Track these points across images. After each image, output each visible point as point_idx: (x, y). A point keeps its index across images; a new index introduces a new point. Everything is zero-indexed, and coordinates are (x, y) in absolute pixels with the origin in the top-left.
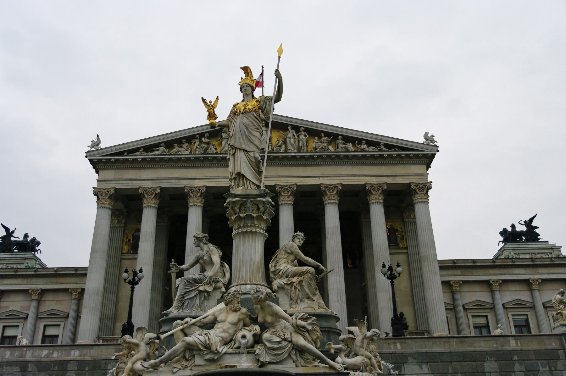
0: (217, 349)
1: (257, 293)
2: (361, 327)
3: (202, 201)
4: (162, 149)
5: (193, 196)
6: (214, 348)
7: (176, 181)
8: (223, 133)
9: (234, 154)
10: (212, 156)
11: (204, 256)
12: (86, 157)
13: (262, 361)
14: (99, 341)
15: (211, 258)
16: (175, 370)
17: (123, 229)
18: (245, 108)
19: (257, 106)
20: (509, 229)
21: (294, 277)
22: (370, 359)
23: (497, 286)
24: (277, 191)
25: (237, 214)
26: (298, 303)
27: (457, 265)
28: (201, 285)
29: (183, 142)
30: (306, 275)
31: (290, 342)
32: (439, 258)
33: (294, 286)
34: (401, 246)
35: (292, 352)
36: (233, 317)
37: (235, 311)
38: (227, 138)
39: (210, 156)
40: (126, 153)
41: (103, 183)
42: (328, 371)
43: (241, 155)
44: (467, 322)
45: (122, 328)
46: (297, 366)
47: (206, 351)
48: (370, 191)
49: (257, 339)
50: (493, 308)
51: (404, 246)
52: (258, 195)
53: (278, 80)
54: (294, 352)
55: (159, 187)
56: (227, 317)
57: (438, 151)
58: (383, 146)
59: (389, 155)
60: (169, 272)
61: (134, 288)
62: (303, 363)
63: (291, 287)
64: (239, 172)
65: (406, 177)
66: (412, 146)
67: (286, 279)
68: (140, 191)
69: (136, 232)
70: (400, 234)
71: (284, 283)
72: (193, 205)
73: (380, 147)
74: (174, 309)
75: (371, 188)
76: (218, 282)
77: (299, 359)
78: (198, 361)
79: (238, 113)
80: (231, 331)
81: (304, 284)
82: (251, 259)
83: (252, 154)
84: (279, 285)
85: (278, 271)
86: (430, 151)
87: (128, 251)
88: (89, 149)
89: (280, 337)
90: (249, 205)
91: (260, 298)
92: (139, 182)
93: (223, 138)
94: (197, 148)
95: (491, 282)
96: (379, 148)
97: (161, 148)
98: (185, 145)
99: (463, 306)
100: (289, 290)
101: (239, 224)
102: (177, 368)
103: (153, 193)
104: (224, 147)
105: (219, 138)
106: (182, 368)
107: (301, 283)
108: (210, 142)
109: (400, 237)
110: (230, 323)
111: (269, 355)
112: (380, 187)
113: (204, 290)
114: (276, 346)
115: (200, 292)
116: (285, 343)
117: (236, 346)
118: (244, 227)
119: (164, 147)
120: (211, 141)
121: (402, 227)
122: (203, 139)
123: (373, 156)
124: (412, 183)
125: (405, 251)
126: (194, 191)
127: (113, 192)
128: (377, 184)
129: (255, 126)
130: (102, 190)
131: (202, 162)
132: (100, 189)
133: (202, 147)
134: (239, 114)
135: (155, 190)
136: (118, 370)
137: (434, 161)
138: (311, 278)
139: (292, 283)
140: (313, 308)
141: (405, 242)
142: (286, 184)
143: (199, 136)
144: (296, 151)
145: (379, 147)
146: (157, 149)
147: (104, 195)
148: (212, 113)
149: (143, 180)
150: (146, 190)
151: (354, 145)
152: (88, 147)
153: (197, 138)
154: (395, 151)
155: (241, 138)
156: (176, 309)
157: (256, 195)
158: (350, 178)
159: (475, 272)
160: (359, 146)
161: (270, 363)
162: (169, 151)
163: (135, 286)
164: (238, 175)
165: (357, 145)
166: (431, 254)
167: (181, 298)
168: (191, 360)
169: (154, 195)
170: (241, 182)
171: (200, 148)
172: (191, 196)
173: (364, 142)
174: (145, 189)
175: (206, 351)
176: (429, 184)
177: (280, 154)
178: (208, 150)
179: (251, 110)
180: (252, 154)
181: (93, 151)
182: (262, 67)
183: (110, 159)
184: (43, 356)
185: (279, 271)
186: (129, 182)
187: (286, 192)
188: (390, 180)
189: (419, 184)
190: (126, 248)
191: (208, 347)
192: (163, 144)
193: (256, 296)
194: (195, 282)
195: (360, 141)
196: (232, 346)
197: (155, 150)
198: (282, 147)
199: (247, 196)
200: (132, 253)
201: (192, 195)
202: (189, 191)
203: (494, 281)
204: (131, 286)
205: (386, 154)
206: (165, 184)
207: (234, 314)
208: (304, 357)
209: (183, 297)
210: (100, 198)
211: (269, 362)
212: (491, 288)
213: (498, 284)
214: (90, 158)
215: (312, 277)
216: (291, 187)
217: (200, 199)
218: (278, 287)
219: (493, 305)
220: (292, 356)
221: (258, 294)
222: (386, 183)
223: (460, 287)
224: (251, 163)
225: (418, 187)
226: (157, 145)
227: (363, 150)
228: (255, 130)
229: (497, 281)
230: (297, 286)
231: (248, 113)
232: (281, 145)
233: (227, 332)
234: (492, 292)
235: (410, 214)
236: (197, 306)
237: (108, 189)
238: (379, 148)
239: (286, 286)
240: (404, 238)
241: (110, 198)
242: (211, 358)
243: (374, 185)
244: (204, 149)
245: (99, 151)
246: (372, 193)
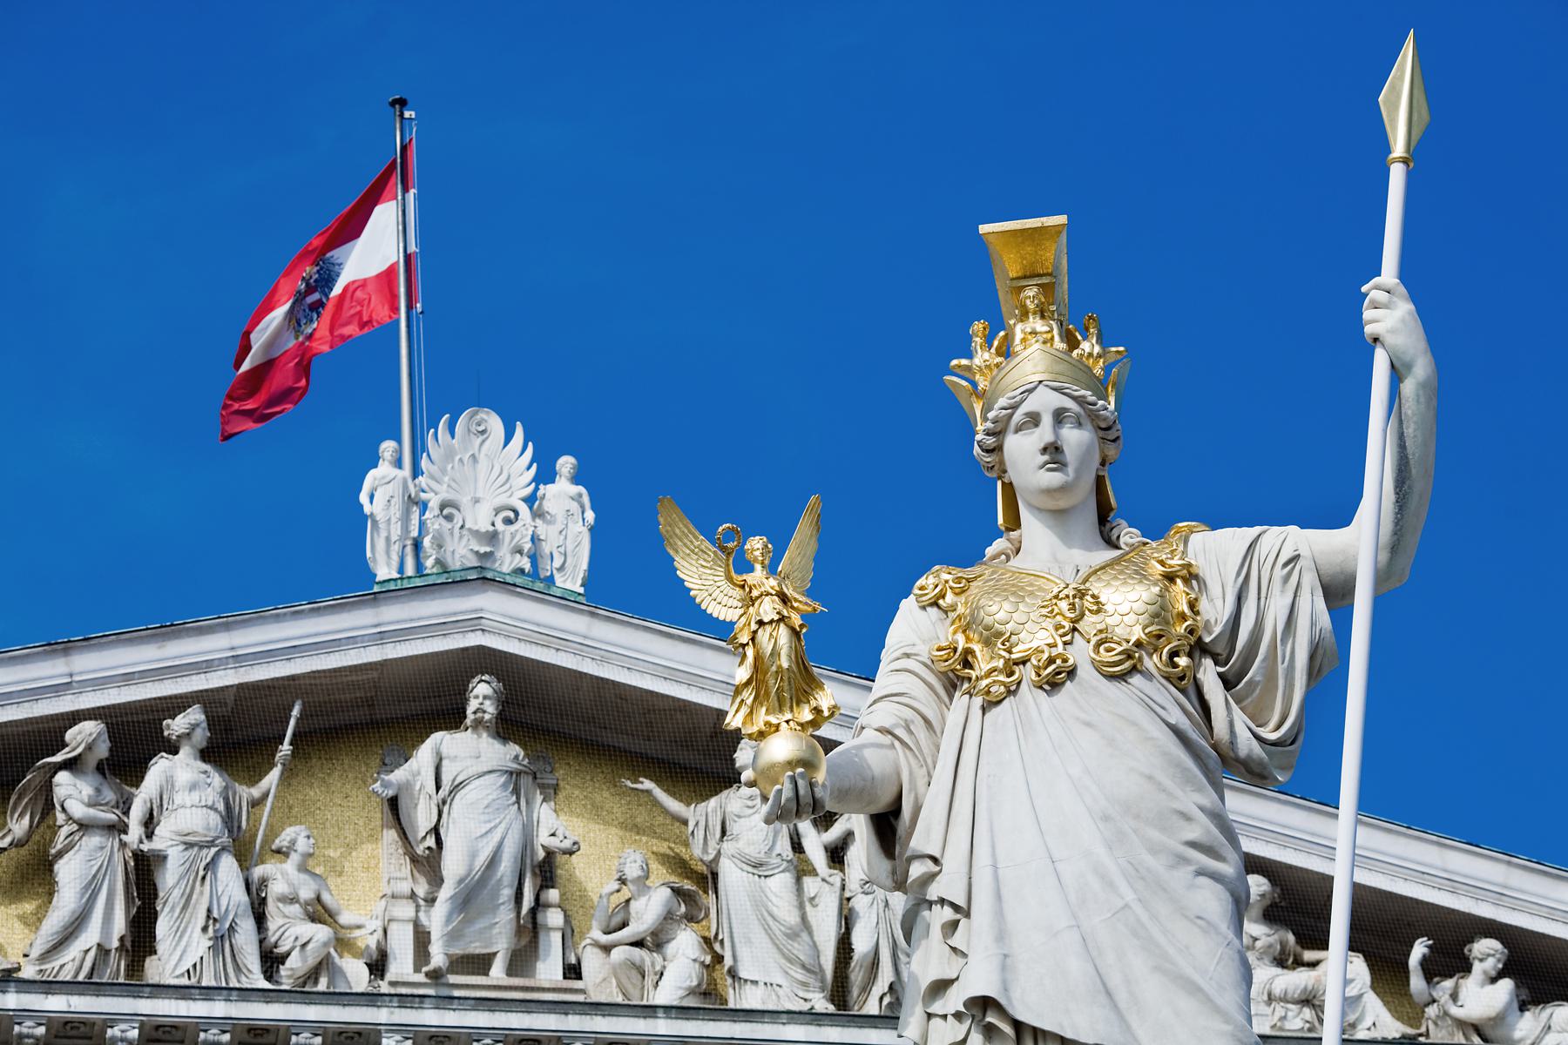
8: (70, 765)
79: (1002, 678)
105: (26, 821)
144: (822, 1004)
198: (670, 949)
228: (1185, 860)
232: (654, 934)
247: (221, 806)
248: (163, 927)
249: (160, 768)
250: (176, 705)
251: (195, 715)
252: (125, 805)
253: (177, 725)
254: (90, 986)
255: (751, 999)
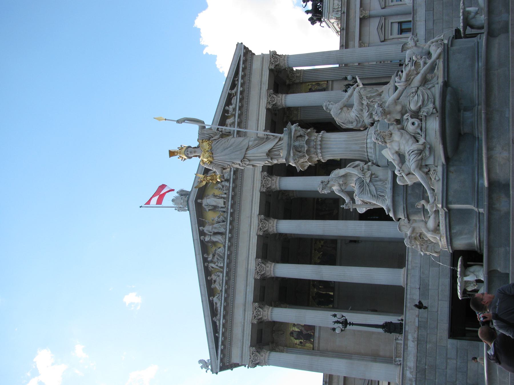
0: (422, 145)
1: (378, 113)
2: (407, 48)
3: (270, 263)
4: (215, 299)
5: (264, 272)
6: (421, 147)
7: (248, 287)
8: (205, 240)
9: (249, 160)
10: (226, 251)
11: (339, 184)
12: (217, 373)
13: (432, 109)
14: (397, 361)
15: (342, 176)
16: (437, 178)
17: (289, 348)
18: (208, 151)
19: (206, 141)
20: (310, 15)
21: (363, 104)
22: (432, 43)
23: (365, 12)
24: (266, 190)
25: (304, 154)
26: (385, 101)
27: (344, 44)
28: (365, 181)
29: (210, 279)
30: (361, 94)
31: (418, 88)
32: (339, 49)
33: (370, 103)
34: (325, 86)
35: (426, 87)
36: (396, 136)
37: (391, 134)
38: (211, 236)
39: (226, 253)
40: (217, 335)
41: (244, 359)
42: (441, 60)
43: (250, 153)
44: (396, 39)
45: (388, 333)
46: (438, 84)
47: (423, 154)
48: (273, 105)
49: (416, 114)
50: (385, 17)
51: (325, 83)
52: (289, 135)
53: (186, 121)
54: (426, 86)
55: (252, 303)
56: (396, 141)
57: (242, 43)
58: (232, 91)
59: (241, 86)
60: (351, 210)
61: (350, 323)
62: (435, 79)
63: (371, 106)
64: (267, 154)
65: (264, 73)
66: (235, 65)
67: (364, 111)
68: (255, 322)
69: (293, 336)
70: (314, 87)
71: (367, 112)
72: (273, 271)
73: (233, 94)
74: (384, 204)
75: (270, 104)
76: (363, 167)
77: (432, 82)
78: (430, 161)
80: (408, 137)
81: (370, 95)
82: (344, 141)
83: (251, 143)
84: (369, 117)
85: (357, 118)
86: (242, 50)
87: (312, 344)
88: (209, 371)
89: (414, 97)
90: (297, 143)
91: (382, 111)
92: (246, 323)
93: (210, 240)
94: (217, 266)
95: (362, 17)
96: (234, 95)
97: (214, 300)
98: (214, 277)
99: (381, 42)
100: (373, 108)
101: (312, 153)
102: (435, 177)
103: (258, 309)
104: (219, 239)
106: (436, 173)
107: (368, 98)
108: (213, 253)
109: (317, 87)
110: (401, 139)
111: (427, 105)
112: (270, 96)
113: (370, 178)
114: (421, 98)
115: (370, 181)
116: (419, 92)
117: (419, 131)
118: (316, 148)
119: (214, 297)
120: (212, 252)
121: (307, 84)
122: (209, 259)
123: (241, 100)
124: (269, 67)
125: (330, 83)
126: (259, 270)
127: (254, 348)
128: (268, 98)
129: (225, 142)
130: (251, 359)
131: (231, 269)
132: (250, 362)
133: (217, 260)
134: (212, 157)
135: (255, 308)
136: (433, 251)
137: (250, 49)
138: (365, 90)
139: (368, 105)
140: (389, 89)
141: (323, 83)
142: (260, 182)
143: (206, 263)
145: (232, 95)
146: (215, 305)
147: (256, 358)
148: (210, 177)
149: (244, 319)
150: (255, 317)
151: (228, 117)
152: (207, 372)
153: (208, 265)
154: (238, 80)
155: (236, 153)
156: (384, 203)
157: (289, 138)
158: (260, 122)
159: (351, 30)
160: (230, 113)
161: (434, 103)
162: (218, 294)
163: (348, 322)
164: (268, 156)
165: (229, 115)
166: (336, 54)
167: (375, 198)
168: (429, 168)
169: (260, 309)
170: (275, 153)
171: (218, 263)
172: (264, 274)
173: (227, 108)
174: (254, 318)
175: (423, 154)
176: (272, 54)
177: (231, 185)
178: (221, 254)
179: (210, 146)
180: (251, 143)
181: (211, 367)
182: (142, 207)
183: (222, 350)
184: (411, 376)
185: (357, 117)
186: (245, 333)
187: (268, 182)
188: (265, 87)
189: (270, 61)
190: (308, 345)
191: (420, 152)
192: (211, 299)
193: (380, 114)
194: (362, 187)
195: (225, 111)
196: (420, 135)
197: (216, 307)
199: (289, 146)
200: (314, 340)
201: (263, 273)
202: (259, 275)
203: (361, 14)
204: (348, 325)
205: (240, 89)
206: (250, 297)
207: (393, 135)
208: (430, 79)
209: (375, 196)
210: (257, 362)
211: (433, 104)
212: (367, 17)
213: (364, 11)
214: (218, 370)
215: (363, 89)
216: (264, 177)
217: (268, 265)
218: (371, 118)
219: (382, 17)
220: (429, 87)
221: (379, 112)
222: (268, 89)
223: (365, 43)
224: (258, 145)
225: (273, 62)
226: (211, 304)
227: (234, 109)
228: (229, 142)
229: (361, 12)
230: (371, 100)
231: (212, 149)
233: (408, 140)
234: (370, 17)
235: (296, 76)
236: (383, 184)
237: (250, 353)
238: (234, 95)
239: (370, 111)
240: (318, 83)
241: (259, 352)
242: (429, 149)
243: (268, 101)
244: (219, 258)
245: (213, 360)
246: (275, 104)
247: (209, 226)
248: (220, 231)
249: (205, 231)
250: (199, 230)
251: (200, 228)
252: (209, 235)
253: (201, 229)
254: (226, 238)
255: (229, 177)
